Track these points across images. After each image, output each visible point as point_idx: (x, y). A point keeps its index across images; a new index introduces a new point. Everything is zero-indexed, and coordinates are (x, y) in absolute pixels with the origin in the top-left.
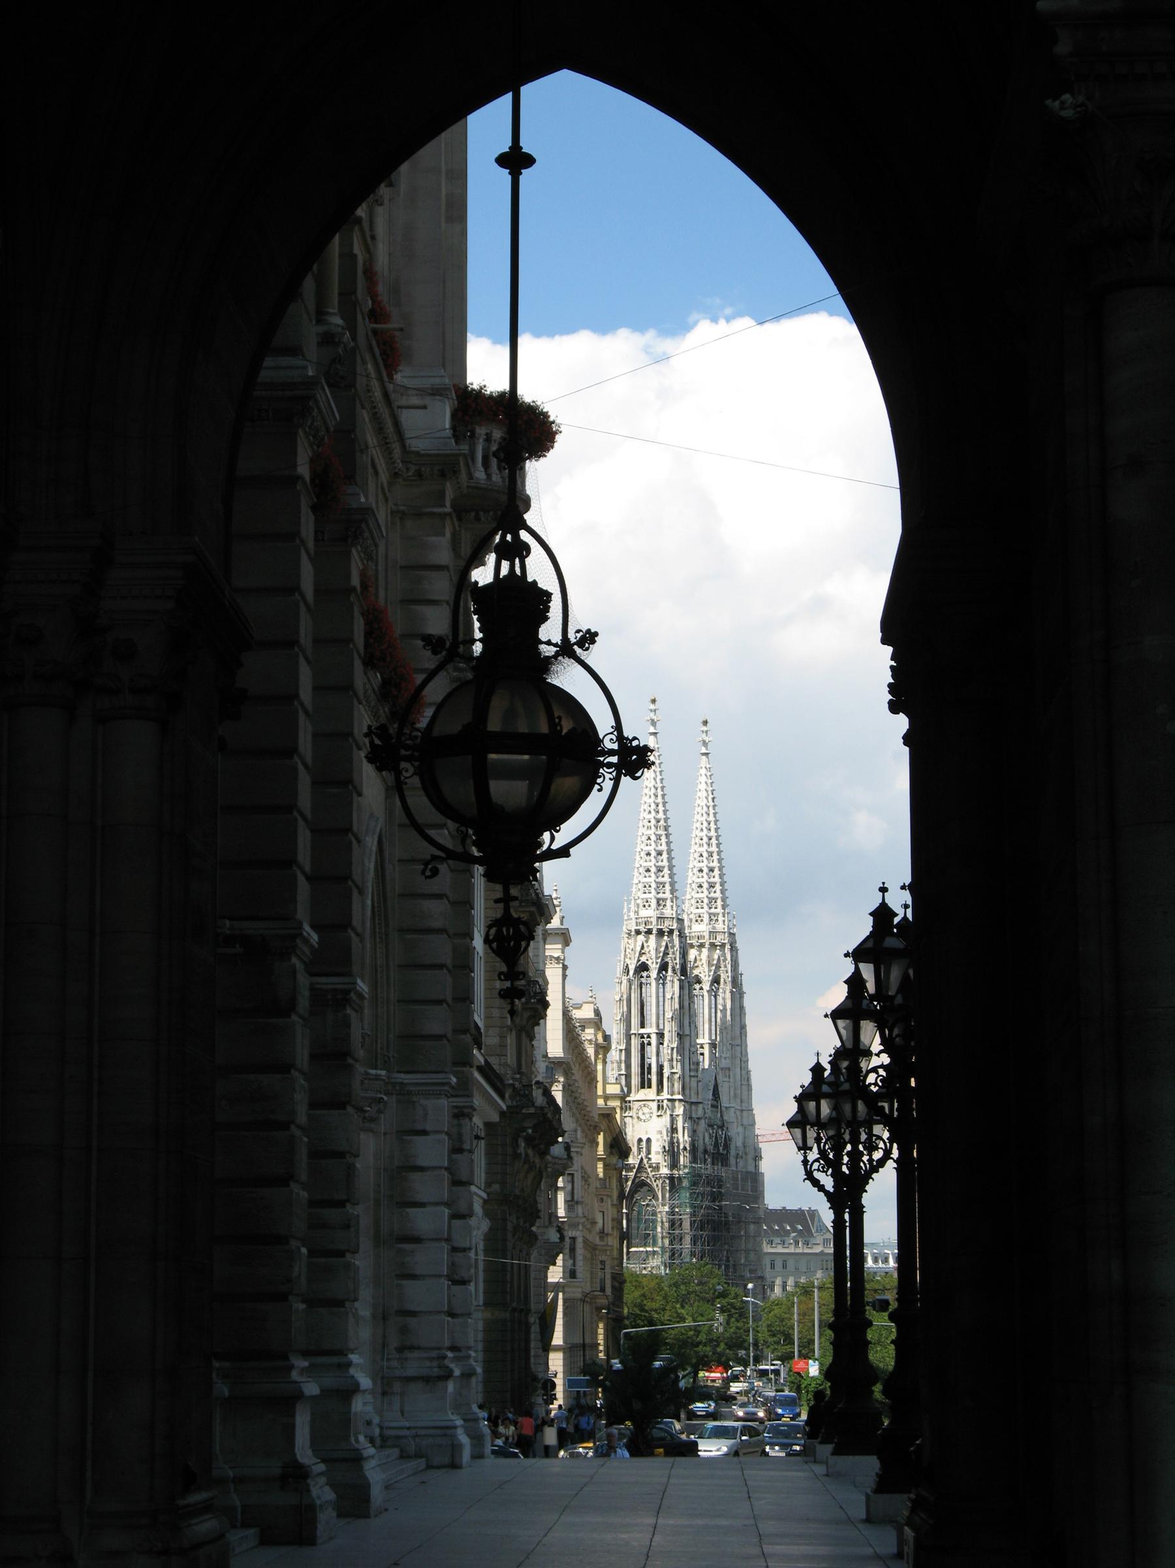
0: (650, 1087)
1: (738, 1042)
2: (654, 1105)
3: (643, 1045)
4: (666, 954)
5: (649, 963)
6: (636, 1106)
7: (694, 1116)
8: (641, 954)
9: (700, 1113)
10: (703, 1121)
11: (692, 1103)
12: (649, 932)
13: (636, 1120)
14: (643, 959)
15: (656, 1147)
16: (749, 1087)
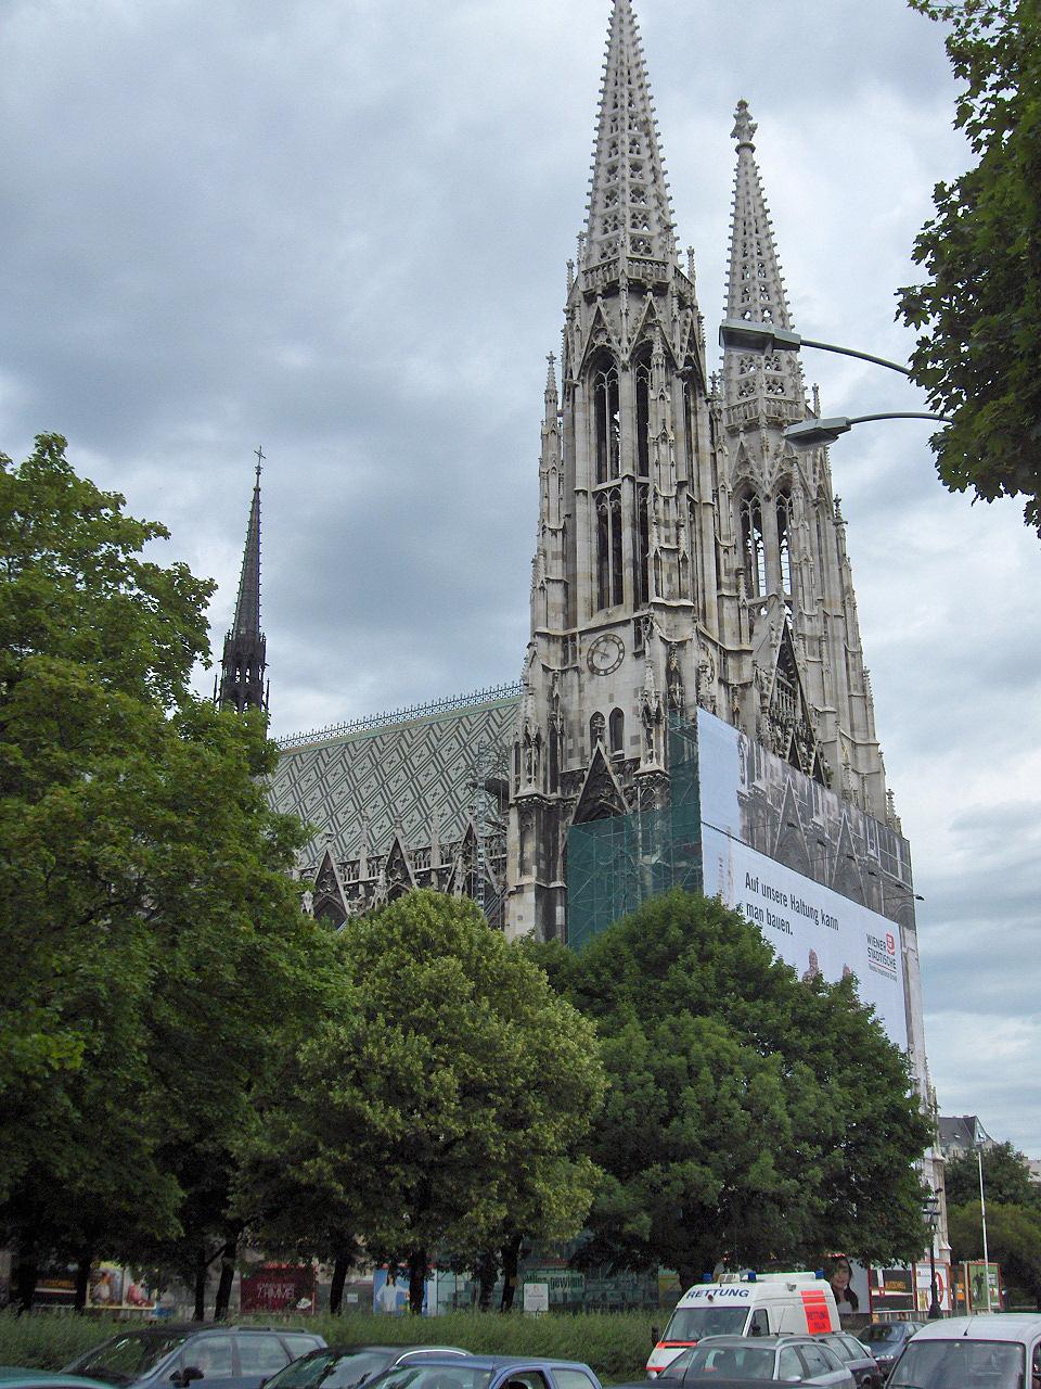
0: (619, 600)
1: (840, 612)
2: (627, 634)
3: (602, 518)
4: (647, 326)
5: (615, 346)
6: (585, 645)
7: (733, 681)
8: (595, 332)
9: (747, 674)
10: (755, 693)
11: (725, 653)
12: (612, 291)
13: (587, 674)
14: (601, 341)
15: (632, 726)
16: (867, 702)
